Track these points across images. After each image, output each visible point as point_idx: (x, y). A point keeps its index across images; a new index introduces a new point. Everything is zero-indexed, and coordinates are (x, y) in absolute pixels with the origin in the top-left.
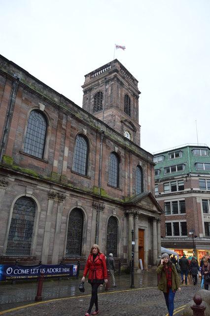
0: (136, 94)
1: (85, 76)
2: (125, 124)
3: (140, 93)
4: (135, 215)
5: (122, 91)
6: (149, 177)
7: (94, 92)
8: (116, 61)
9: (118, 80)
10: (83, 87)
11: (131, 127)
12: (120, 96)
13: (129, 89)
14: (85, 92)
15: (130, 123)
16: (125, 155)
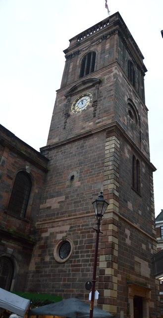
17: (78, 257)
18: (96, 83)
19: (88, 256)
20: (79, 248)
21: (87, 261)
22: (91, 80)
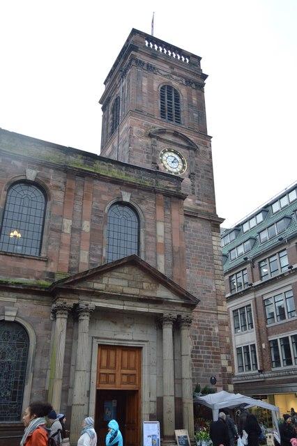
0: (197, 81)
2: (159, 138)
4: (74, 315)
6: (161, 228)
8: (134, 32)
9: (140, 63)
10: (101, 102)
11: (185, 144)
12: (145, 90)
13: (174, 74)
14: (104, 109)
15: (176, 134)
16: (65, 183)
17: (198, 352)
18: (192, 149)
19: (209, 353)
20: (199, 343)
21: (209, 357)
22: (186, 139)
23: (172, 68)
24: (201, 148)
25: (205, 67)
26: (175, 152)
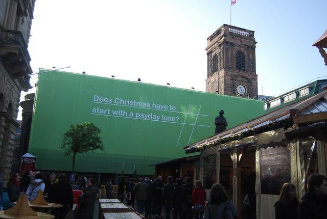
1: (207, 39)
3: (256, 43)
5: (232, 52)
7: (213, 54)
11: (245, 80)
12: (229, 57)
13: (242, 44)
15: (243, 77)
22: (247, 79)
23: (241, 42)
24: (253, 81)
25: (257, 37)
26: (242, 85)
